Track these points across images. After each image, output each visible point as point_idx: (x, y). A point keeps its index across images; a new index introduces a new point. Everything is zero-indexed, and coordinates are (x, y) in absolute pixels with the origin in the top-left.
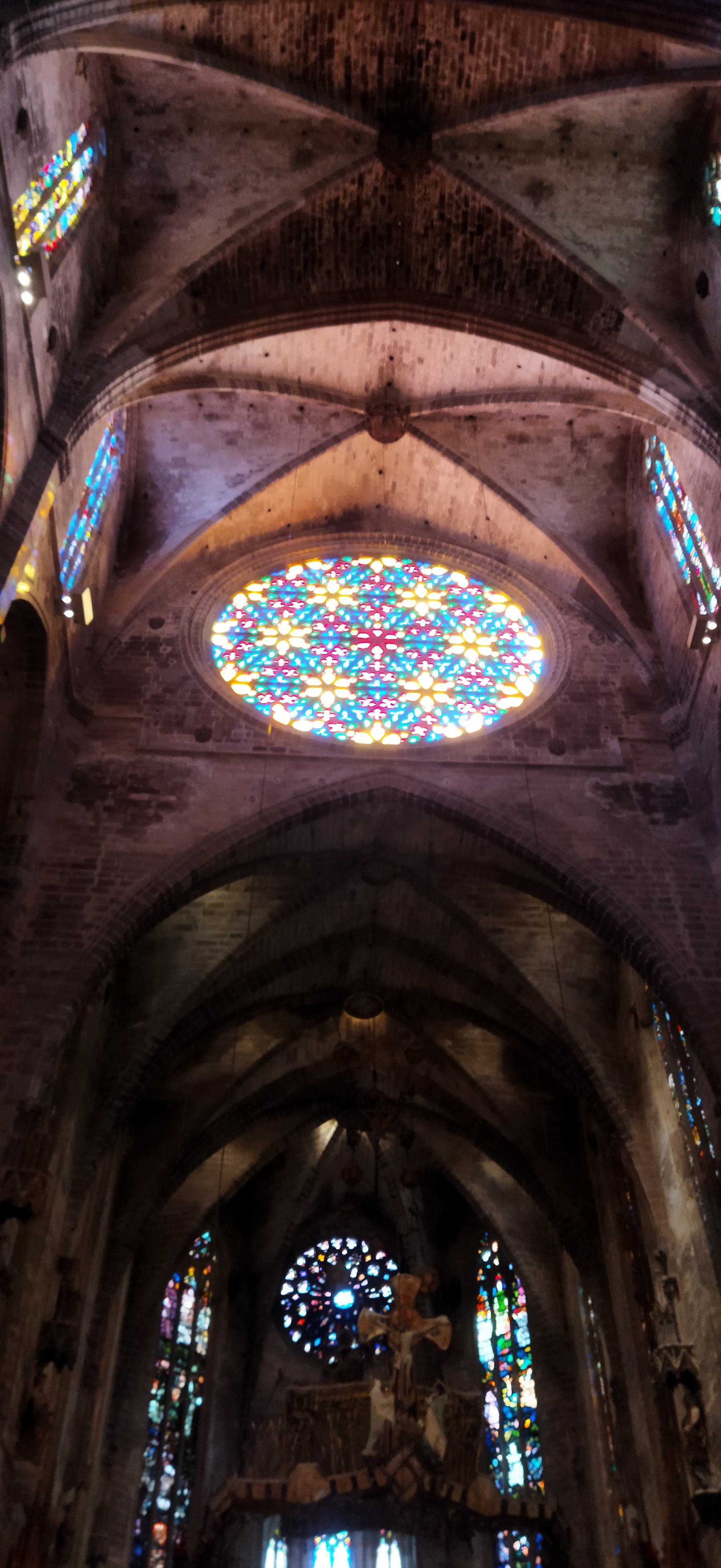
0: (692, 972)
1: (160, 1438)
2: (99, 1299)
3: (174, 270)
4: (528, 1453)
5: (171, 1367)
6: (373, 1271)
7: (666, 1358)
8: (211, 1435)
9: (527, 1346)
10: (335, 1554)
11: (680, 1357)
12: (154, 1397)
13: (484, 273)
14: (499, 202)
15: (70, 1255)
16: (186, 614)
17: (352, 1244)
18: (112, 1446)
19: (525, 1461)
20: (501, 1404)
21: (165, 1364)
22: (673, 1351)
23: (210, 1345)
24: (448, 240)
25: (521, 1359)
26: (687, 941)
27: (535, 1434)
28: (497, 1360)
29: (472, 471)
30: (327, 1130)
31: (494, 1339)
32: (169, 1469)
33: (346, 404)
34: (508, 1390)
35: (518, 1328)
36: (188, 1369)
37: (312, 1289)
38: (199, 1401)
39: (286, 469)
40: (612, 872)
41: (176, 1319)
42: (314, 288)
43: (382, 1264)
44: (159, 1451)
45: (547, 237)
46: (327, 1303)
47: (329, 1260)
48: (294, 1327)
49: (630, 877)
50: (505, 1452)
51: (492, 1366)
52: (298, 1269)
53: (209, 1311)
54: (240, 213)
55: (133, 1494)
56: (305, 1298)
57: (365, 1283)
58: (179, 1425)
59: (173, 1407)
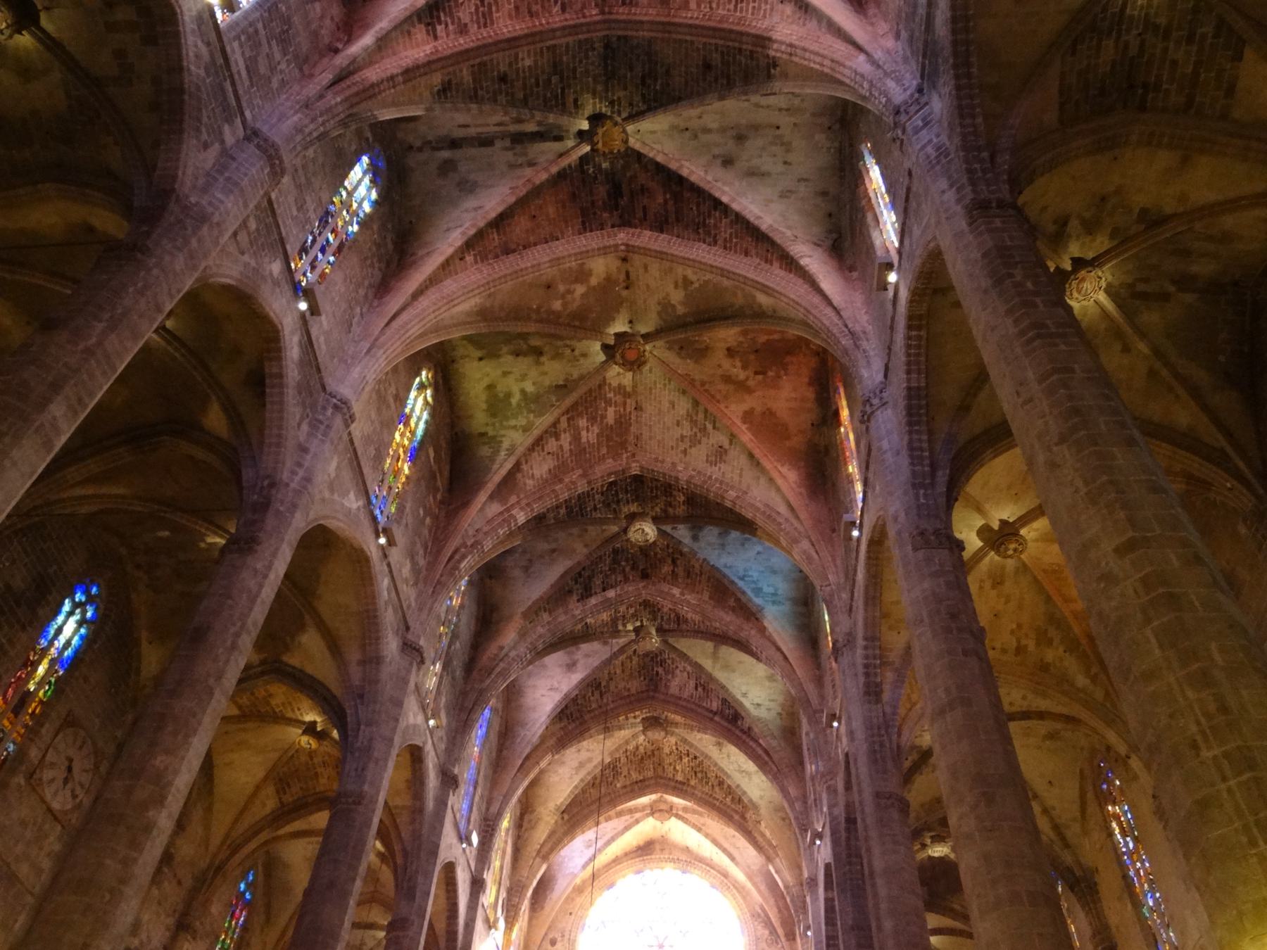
3: (552, 805)
13: (699, 775)
14: (703, 753)
16: (567, 934)
24: (681, 758)
29: (707, 835)
33: (640, 811)
39: (613, 839)
42: (618, 785)
45: (726, 773)
54: (581, 765)
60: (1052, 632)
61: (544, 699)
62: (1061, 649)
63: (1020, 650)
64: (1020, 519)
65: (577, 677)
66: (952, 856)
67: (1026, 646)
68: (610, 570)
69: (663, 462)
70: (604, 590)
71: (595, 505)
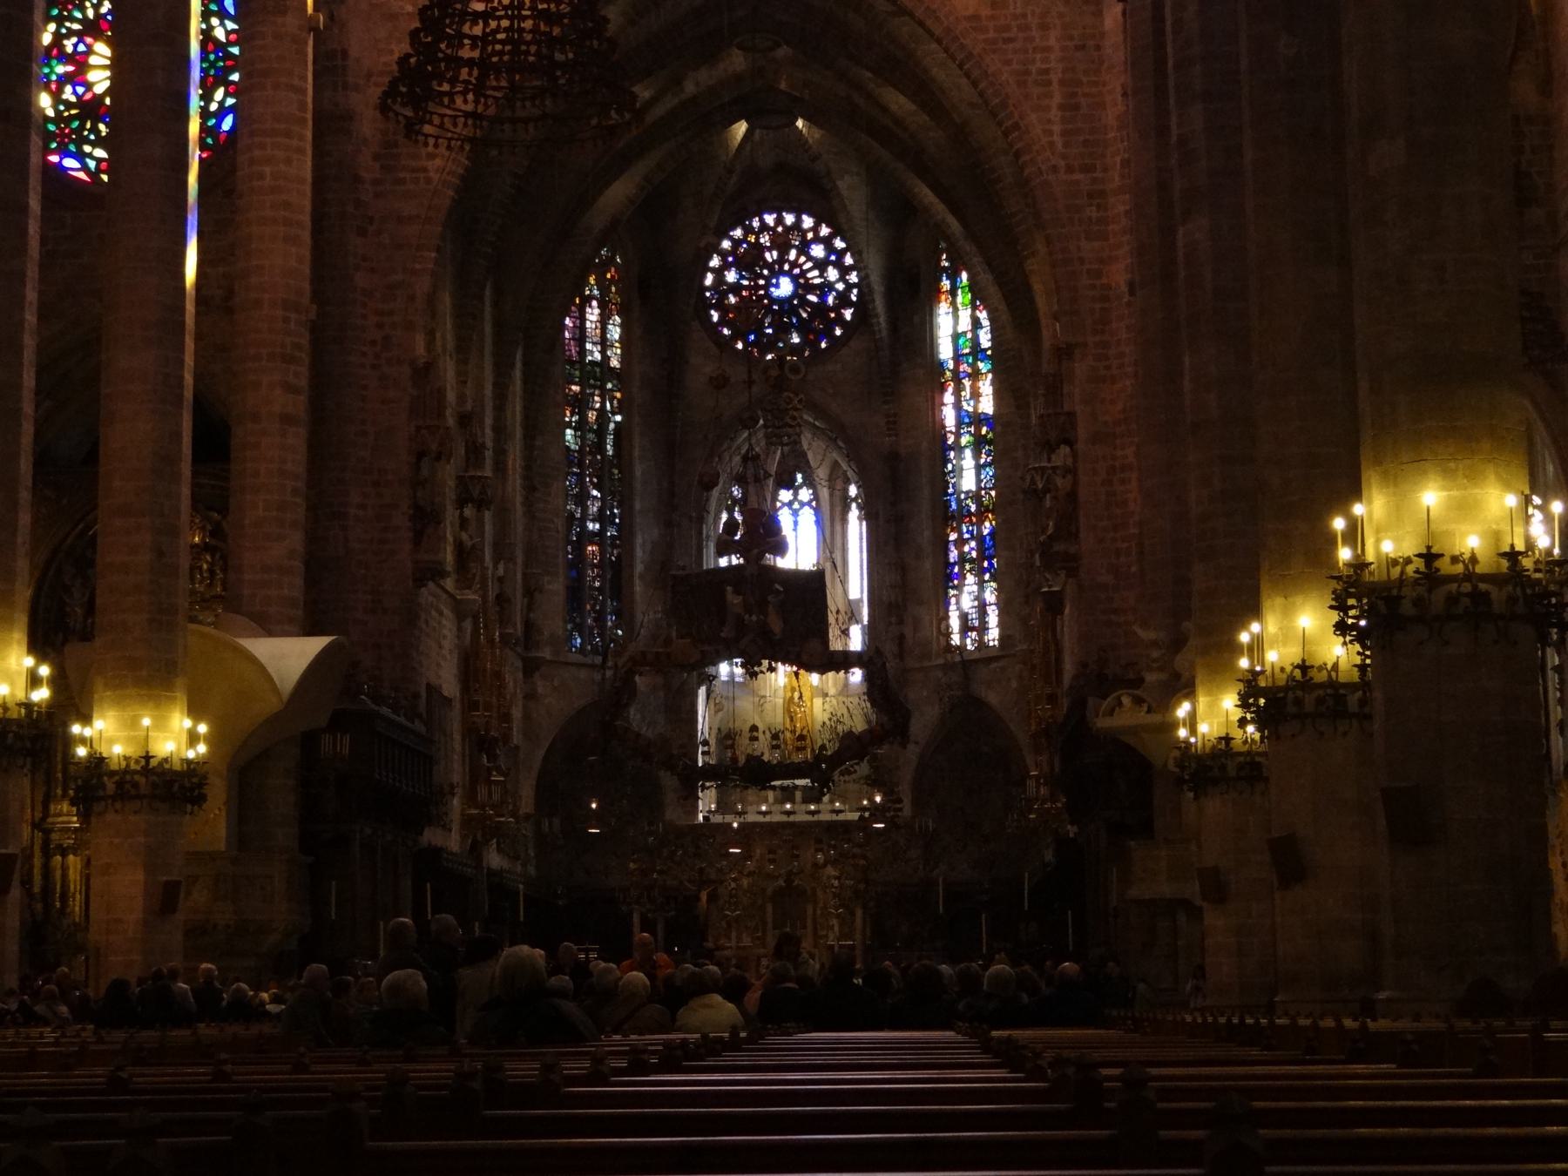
0: (1055, 169)
1: (580, 465)
2: (495, 385)
4: (982, 461)
5: (582, 391)
6: (818, 251)
7: (1033, 477)
8: (636, 453)
9: (989, 349)
10: (799, 519)
11: (1045, 478)
12: (569, 425)
15: (469, 407)
17: (789, 219)
18: (530, 489)
19: (979, 468)
20: (958, 406)
21: (575, 388)
22: (1040, 472)
23: (624, 358)
25: (982, 361)
26: (1057, 128)
27: (990, 443)
28: (958, 357)
30: (741, 128)
31: (956, 337)
32: (595, 493)
34: (966, 394)
35: (982, 328)
36: (602, 388)
37: (742, 277)
38: (618, 418)
40: (991, 35)
41: (581, 336)
43: (827, 242)
44: (581, 476)
46: (762, 292)
47: (762, 241)
48: (723, 322)
49: (1011, 40)
50: (960, 457)
51: (951, 365)
52: (723, 255)
53: (617, 319)
55: (560, 523)
56: (736, 288)
57: (809, 265)
58: (600, 447)
59: (591, 430)
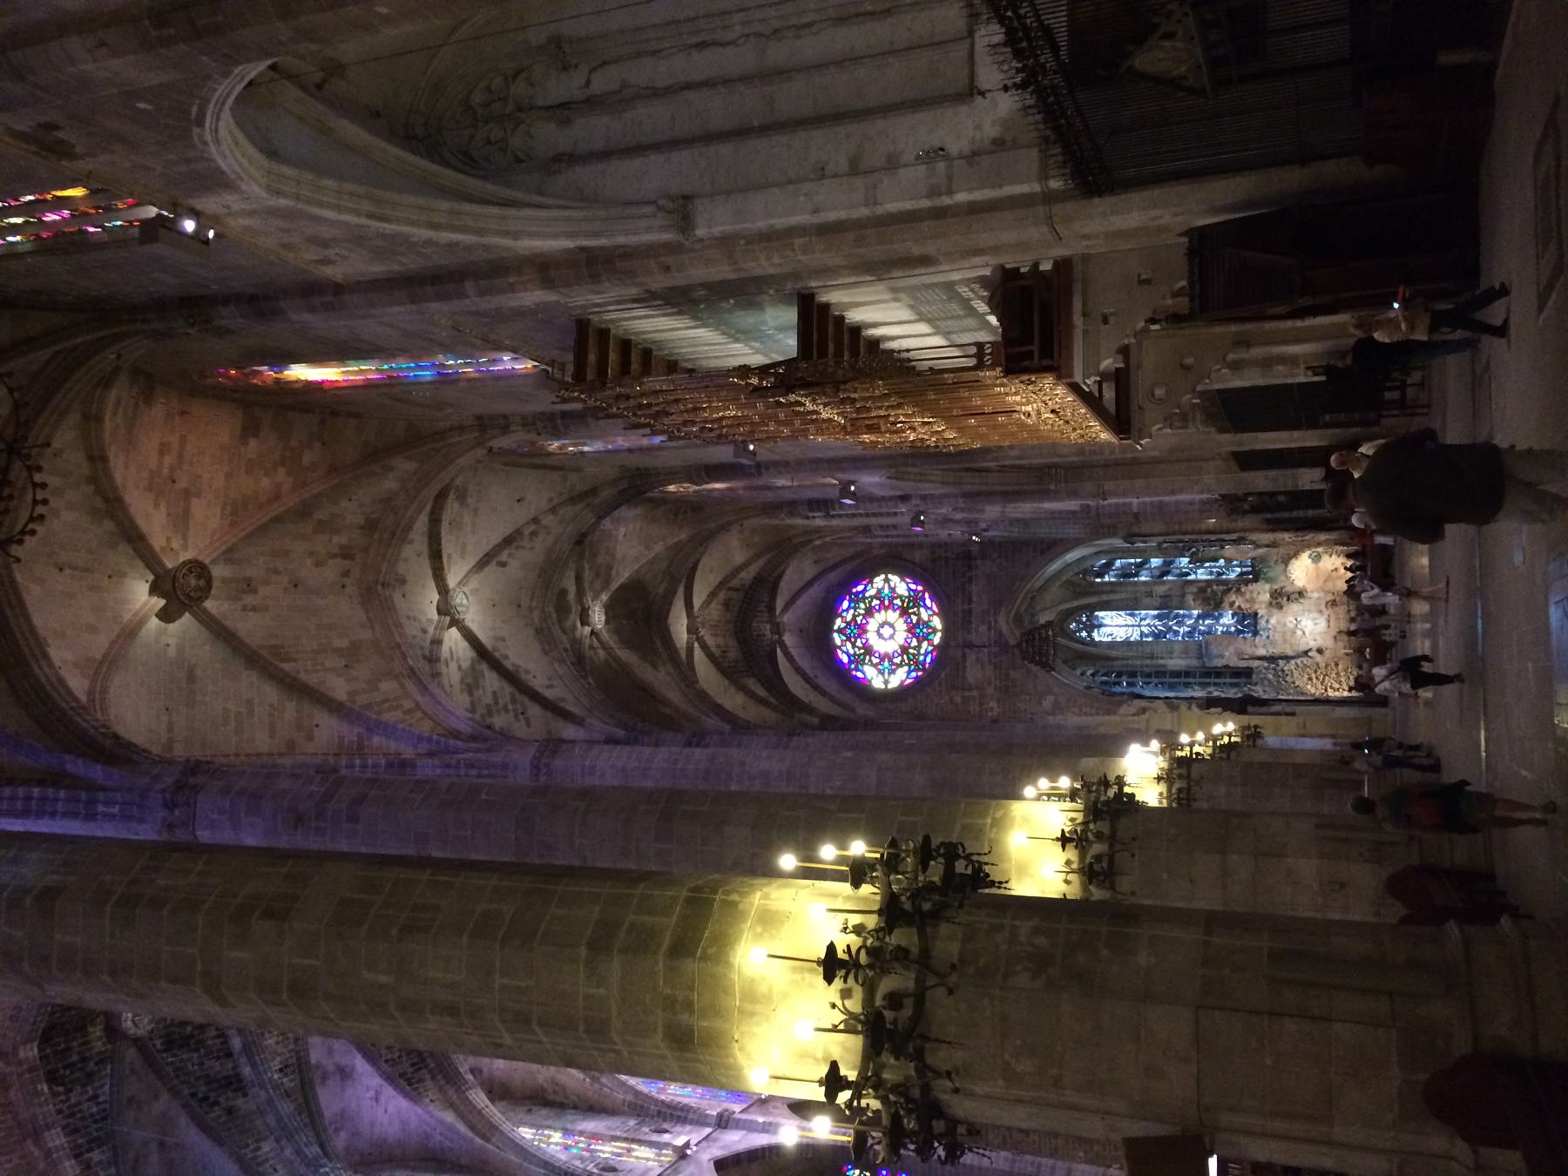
60: (321, 515)
61: (391, 1109)
62: (344, 503)
63: (346, 553)
64: (149, 566)
65: (360, 1064)
66: (604, 597)
67: (341, 547)
68: (197, 1050)
69: (18, 1008)
70: (230, 1055)
71: (90, 1099)
